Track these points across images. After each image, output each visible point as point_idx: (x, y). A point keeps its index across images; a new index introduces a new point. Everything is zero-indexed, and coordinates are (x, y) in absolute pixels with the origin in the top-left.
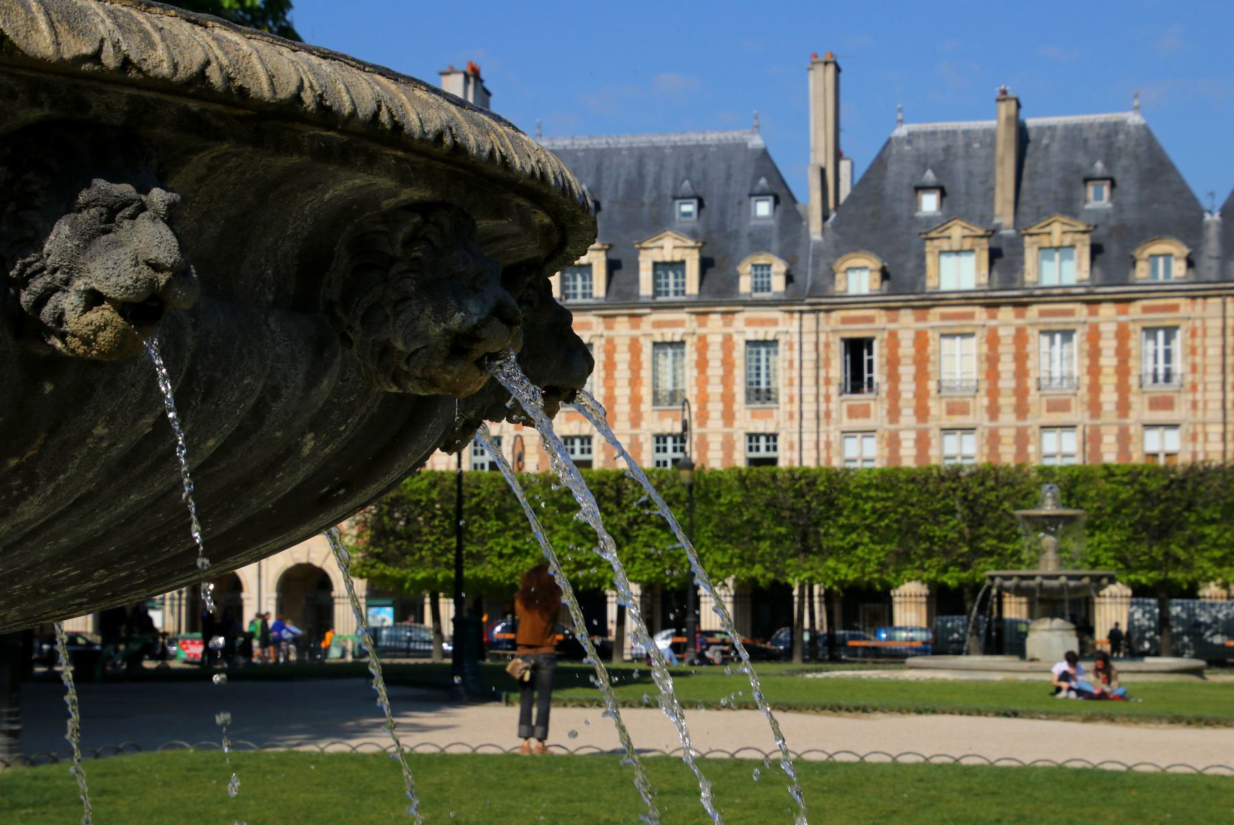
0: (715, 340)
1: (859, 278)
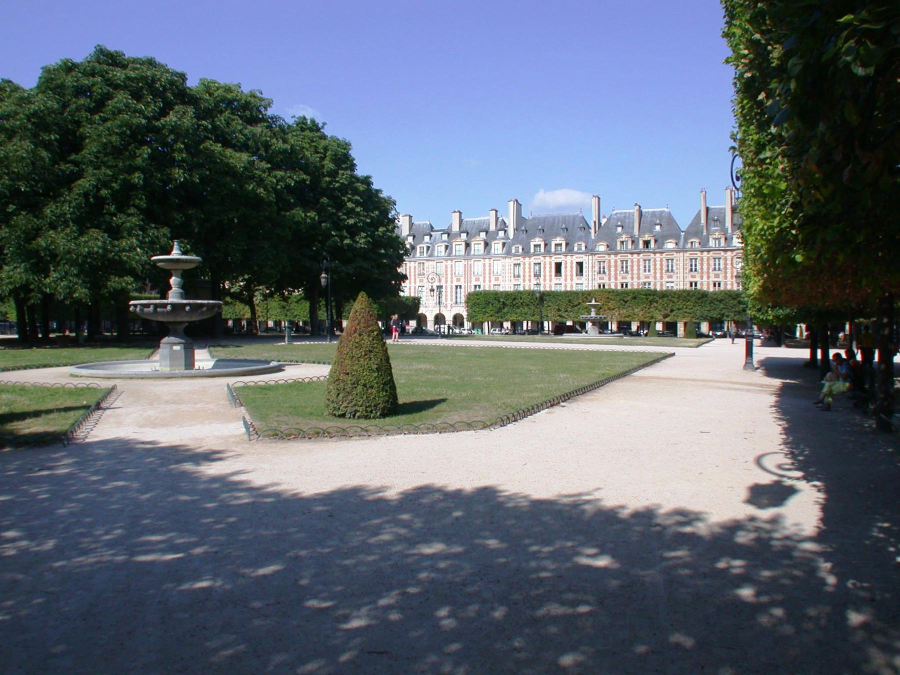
1: (602, 248)
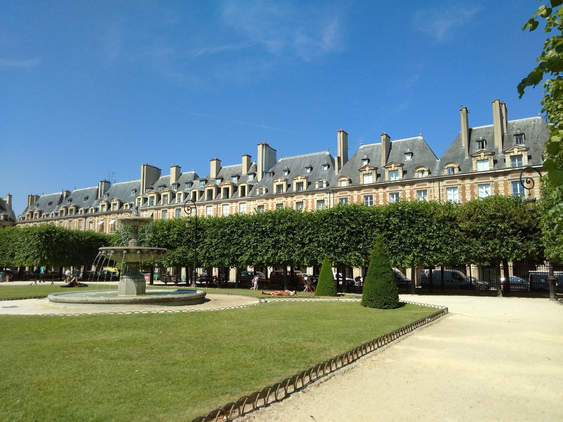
0: (310, 201)
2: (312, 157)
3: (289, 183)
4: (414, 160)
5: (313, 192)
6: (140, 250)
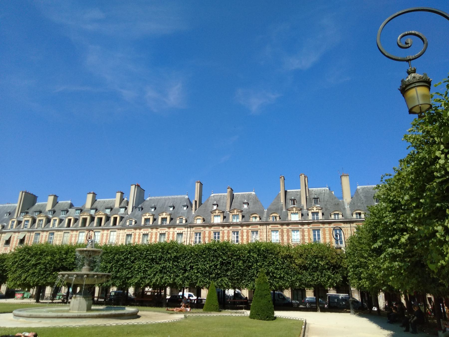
0: (171, 233)
2: (174, 198)
3: (155, 217)
4: (249, 208)
5: (174, 226)
6: (97, 275)
